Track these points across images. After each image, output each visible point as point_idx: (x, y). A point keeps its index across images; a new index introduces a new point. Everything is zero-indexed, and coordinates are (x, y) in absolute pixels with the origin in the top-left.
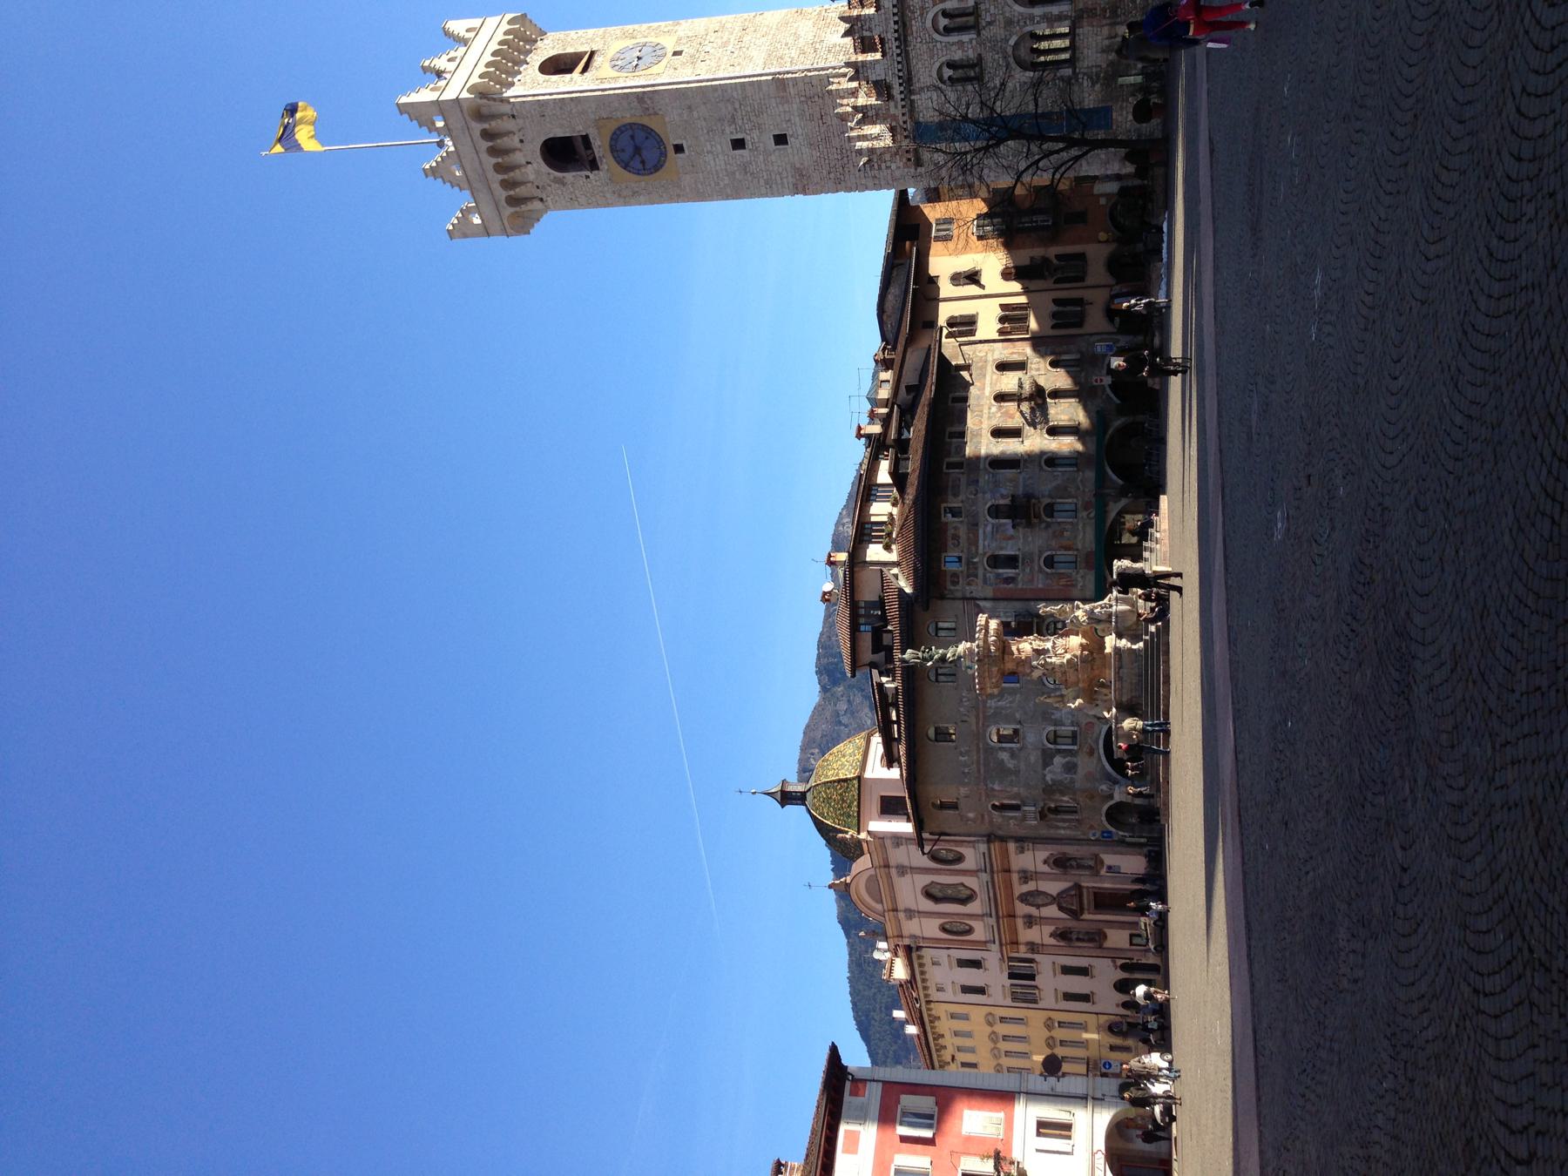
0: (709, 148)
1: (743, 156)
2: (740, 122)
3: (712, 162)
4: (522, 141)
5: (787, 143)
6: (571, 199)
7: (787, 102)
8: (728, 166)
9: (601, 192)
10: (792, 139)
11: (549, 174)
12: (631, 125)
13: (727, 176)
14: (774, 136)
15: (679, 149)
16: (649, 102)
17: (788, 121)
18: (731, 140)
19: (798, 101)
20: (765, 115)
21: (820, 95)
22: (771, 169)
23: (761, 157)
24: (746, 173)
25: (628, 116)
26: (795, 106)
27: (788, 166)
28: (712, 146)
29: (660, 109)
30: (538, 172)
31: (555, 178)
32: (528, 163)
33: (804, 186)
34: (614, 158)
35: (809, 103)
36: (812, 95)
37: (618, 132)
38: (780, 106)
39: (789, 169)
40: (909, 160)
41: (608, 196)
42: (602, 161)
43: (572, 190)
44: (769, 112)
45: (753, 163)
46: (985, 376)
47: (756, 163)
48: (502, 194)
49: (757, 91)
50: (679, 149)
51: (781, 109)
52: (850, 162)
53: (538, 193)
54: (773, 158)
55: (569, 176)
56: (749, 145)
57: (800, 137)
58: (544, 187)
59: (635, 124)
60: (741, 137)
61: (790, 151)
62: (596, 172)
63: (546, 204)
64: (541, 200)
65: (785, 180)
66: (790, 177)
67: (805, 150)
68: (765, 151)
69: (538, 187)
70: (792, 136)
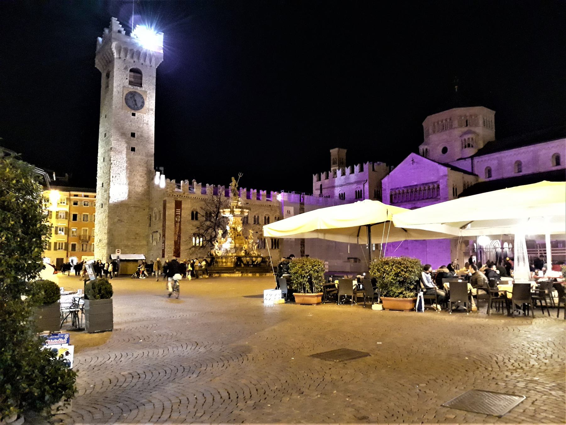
12: (143, 103)
15: (134, 115)
50: (134, 115)
55: (128, 72)
56: (132, 138)
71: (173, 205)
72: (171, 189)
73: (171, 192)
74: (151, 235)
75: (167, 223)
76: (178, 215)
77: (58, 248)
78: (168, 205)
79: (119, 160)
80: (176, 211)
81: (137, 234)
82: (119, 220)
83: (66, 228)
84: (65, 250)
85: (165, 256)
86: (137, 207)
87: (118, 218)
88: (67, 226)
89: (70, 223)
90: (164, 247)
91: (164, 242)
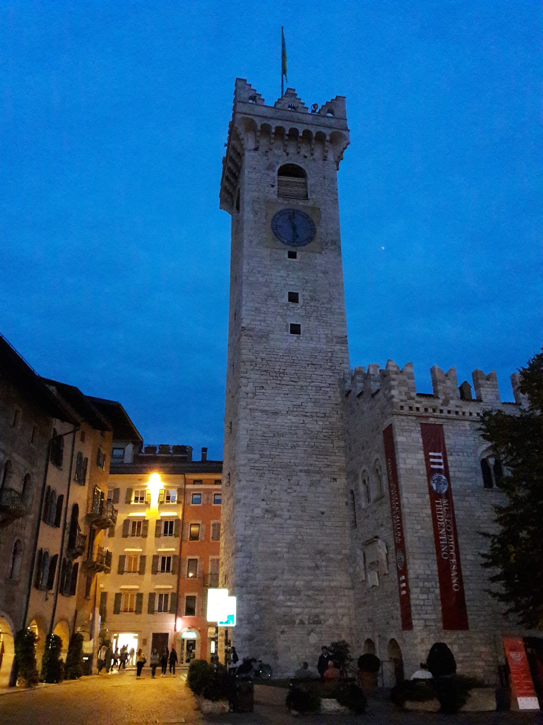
0: (291, 276)
1: (283, 297)
3: (278, 274)
4: (305, 157)
5: (291, 333)
6: (255, 168)
7: (328, 342)
8: (275, 285)
10: (295, 338)
11: (278, 163)
12: (314, 231)
13: (266, 281)
14: (299, 325)
16: (332, 248)
17: (312, 339)
18: (297, 294)
19: (329, 350)
20: (318, 324)
21: (333, 368)
22: (269, 315)
23: (281, 311)
24: (268, 296)
25: (322, 230)
26: (325, 347)
27: (271, 329)
29: (326, 253)
30: (279, 156)
31: (274, 166)
32: (288, 154)
33: (251, 336)
34: (288, 210)
35: (327, 358)
36: (333, 361)
37: (309, 220)
38: (325, 336)
39: (268, 328)
40: (402, 408)
41: (255, 194)
42: (285, 200)
43: (263, 172)
44: (320, 327)
45: (276, 304)
46: (24, 457)
47: (275, 306)
48: (274, 124)
49: (338, 323)
50: (292, 255)
51: (322, 336)
52: (272, 378)
53: (262, 149)
54: (281, 320)
55: (275, 174)
56: (292, 305)
57: (296, 344)
58: (266, 155)
59: (315, 232)
60: (299, 301)
61: (285, 333)
62: (276, 193)
63: (253, 151)
64: (256, 149)
65: (258, 323)
66: (260, 327)
67: (285, 345)
68: (286, 315)
69: (266, 152)
71: (417, 437)
72: (404, 389)
73: (404, 398)
74: (359, 552)
75: (404, 501)
76: (439, 471)
77: (156, 607)
78: (400, 439)
79: (264, 355)
80: (427, 458)
81: (320, 552)
82: (267, 511)
83: (175, 556)
85: (414, 622)
86: (314, 472)
87: (263, 505)
88: (177, 554)
89: (185, 545)
90: (407, 588)
91: (403, 571)
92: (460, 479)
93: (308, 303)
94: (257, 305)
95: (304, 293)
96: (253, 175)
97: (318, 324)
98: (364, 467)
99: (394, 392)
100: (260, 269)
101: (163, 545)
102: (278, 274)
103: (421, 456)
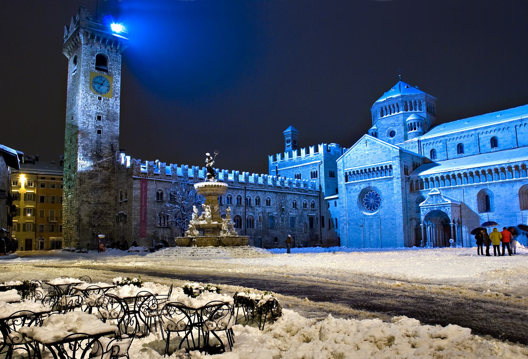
0: (99, 108)
2: (107, 121)
9: (87, 66)
15: (100, 98)
20: (108, 130)
26: (110, 140)
28: (100, 109)
41: (86, 67)
50: (100, 98)
55: (94, 58)
66: (86, 131)
70: (101, 135)
84: (33, 231)
92: (150, 198)
93: (105, 121)
94: (85, 121)
95: (104, 116)
96: (85, 58)
97: (108, 130)
98: (121, 190)
99: (134, 171)
100: (86, 104)
101: (28, 204)
102: (94, 107)
103: (139, 191)
